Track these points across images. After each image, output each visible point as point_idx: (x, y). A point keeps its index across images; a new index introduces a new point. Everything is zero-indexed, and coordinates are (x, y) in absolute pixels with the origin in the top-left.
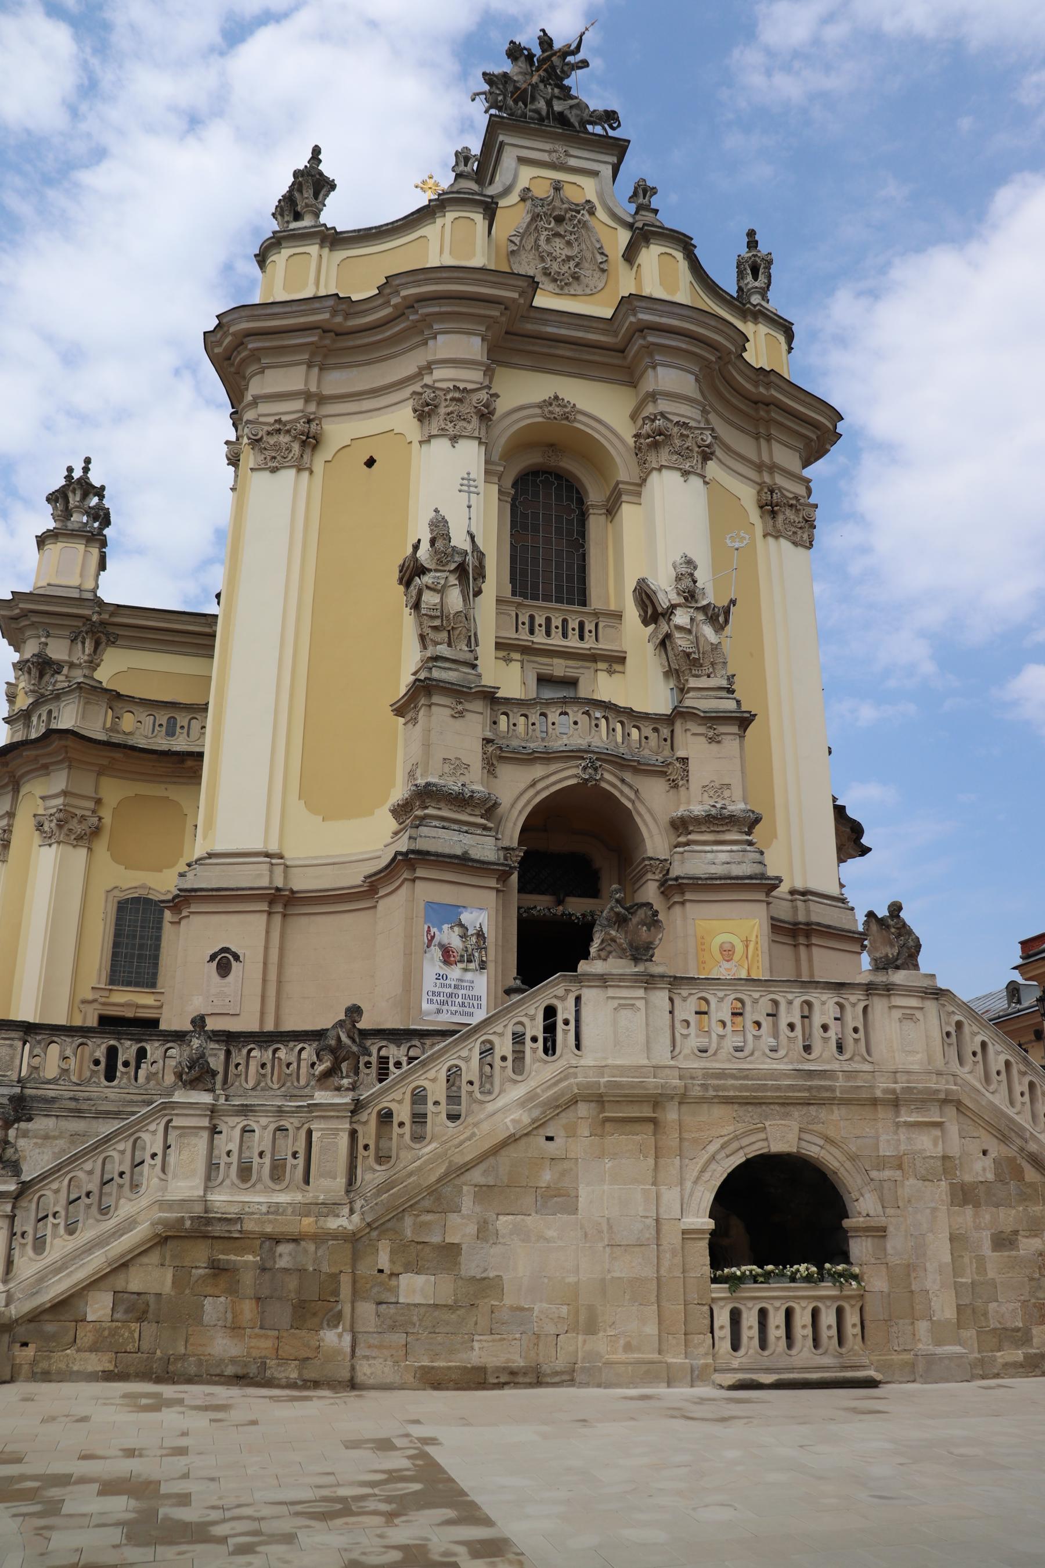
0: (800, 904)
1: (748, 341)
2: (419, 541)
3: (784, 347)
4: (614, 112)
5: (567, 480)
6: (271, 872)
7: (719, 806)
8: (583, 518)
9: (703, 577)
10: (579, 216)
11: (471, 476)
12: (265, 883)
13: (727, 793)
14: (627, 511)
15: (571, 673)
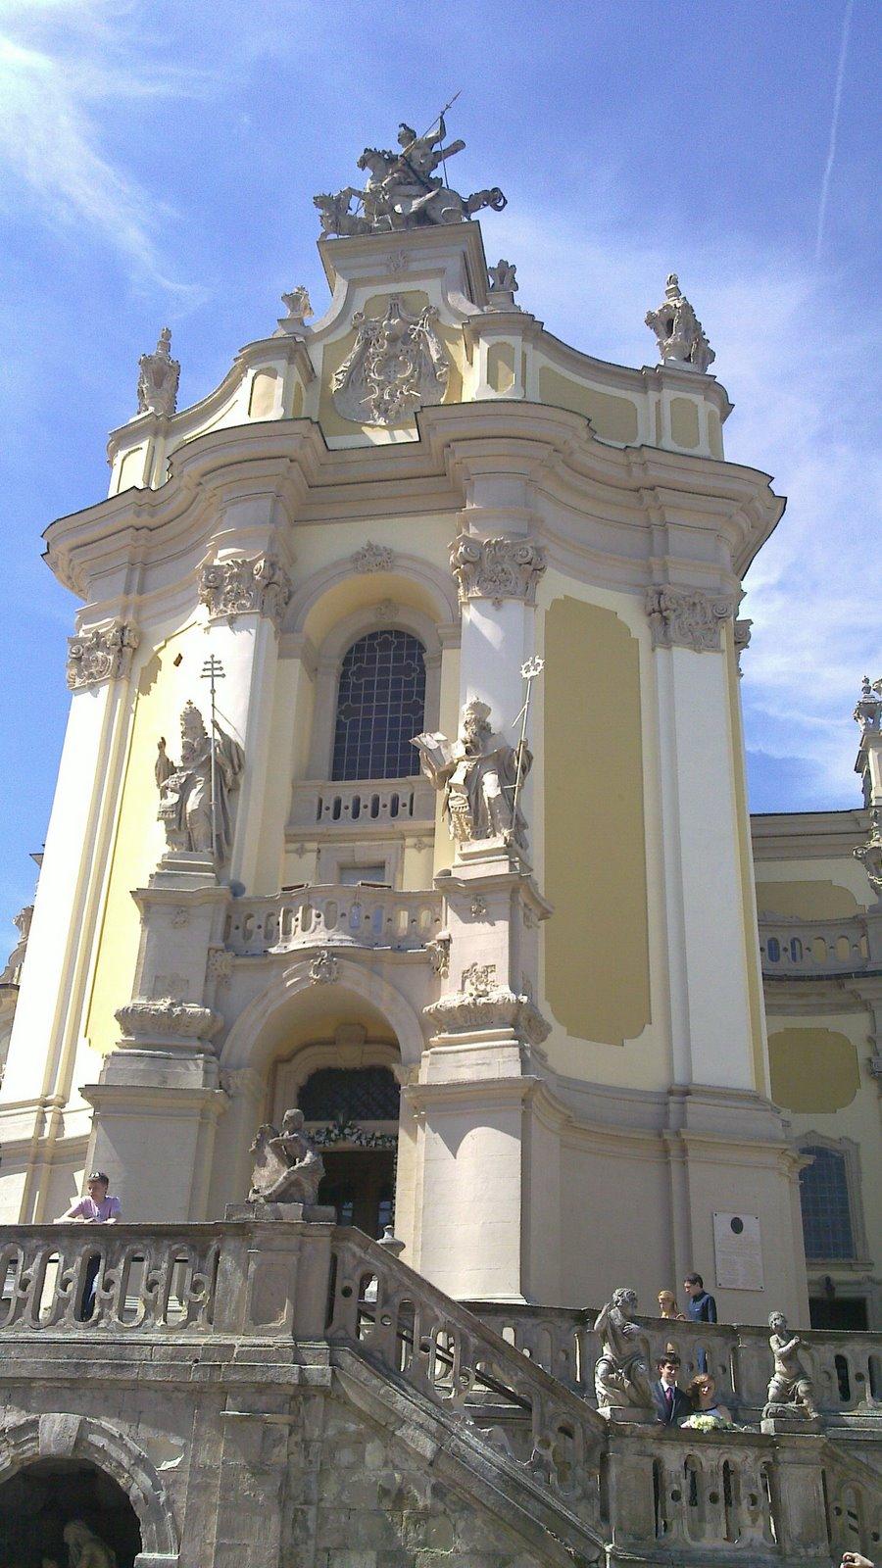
0: (672, 1107)
1: (589, 420)
2: (163, 738)
3: (705, 407)
4: (495, 190)
5: (409, 636)
6: (42, 1121)
7: (475, 993)
8: (423, 672)
9: (494, 720)
10: (418, 328)
11: (215, 659)
12: (28, 1133)
13: (491, 977)
14: (447, 655)
15: (375, 857)
